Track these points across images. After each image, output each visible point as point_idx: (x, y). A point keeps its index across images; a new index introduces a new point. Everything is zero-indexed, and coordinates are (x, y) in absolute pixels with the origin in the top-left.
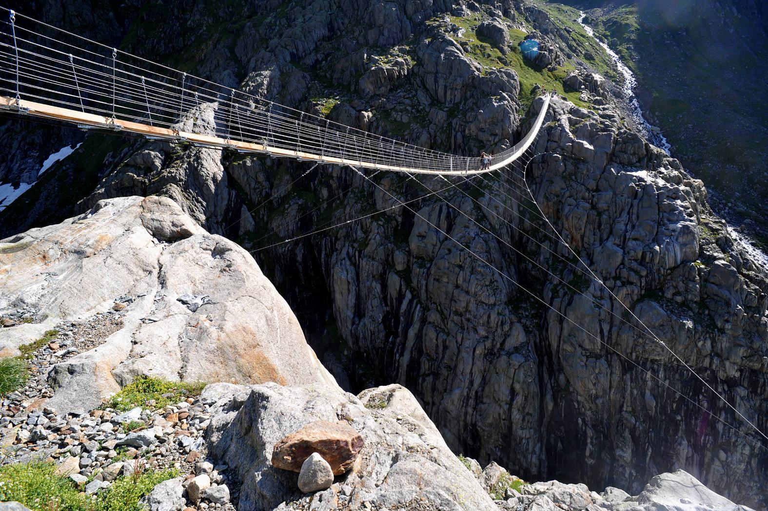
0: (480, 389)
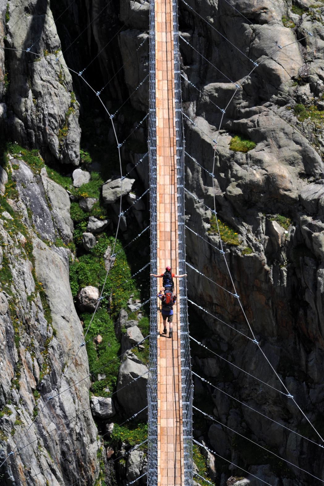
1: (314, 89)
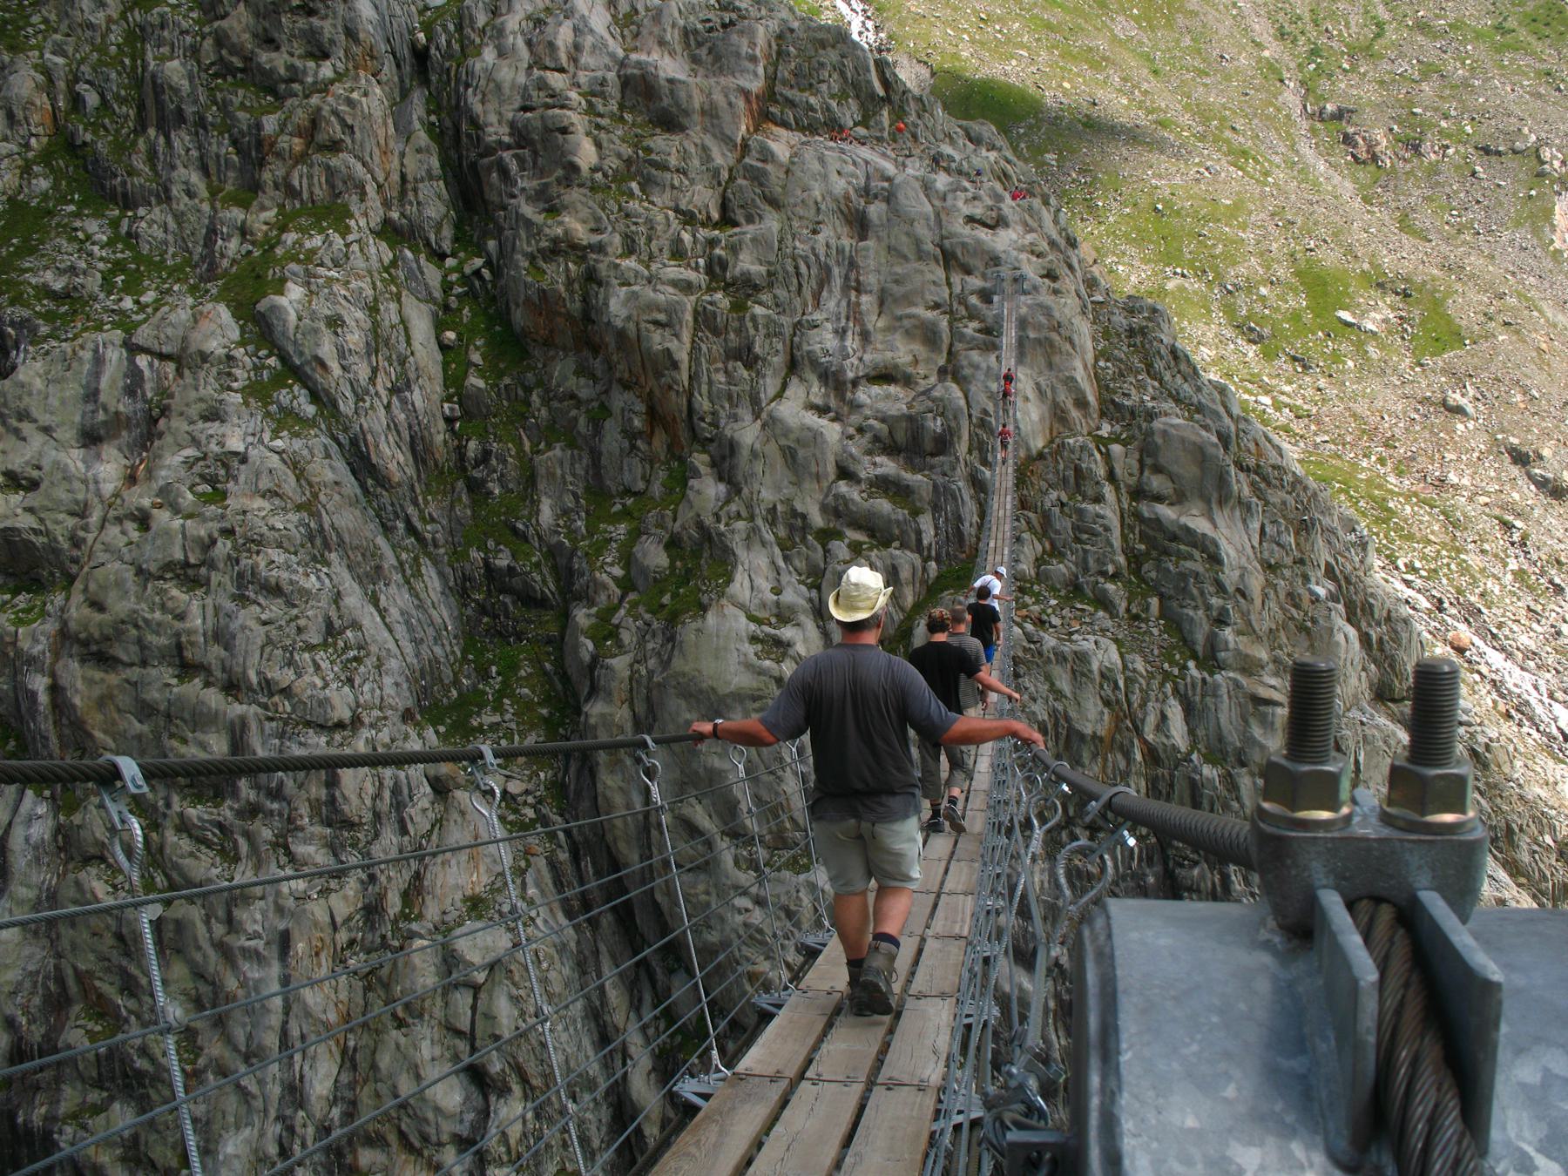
0: (336, 1113)
1: (605, 175)
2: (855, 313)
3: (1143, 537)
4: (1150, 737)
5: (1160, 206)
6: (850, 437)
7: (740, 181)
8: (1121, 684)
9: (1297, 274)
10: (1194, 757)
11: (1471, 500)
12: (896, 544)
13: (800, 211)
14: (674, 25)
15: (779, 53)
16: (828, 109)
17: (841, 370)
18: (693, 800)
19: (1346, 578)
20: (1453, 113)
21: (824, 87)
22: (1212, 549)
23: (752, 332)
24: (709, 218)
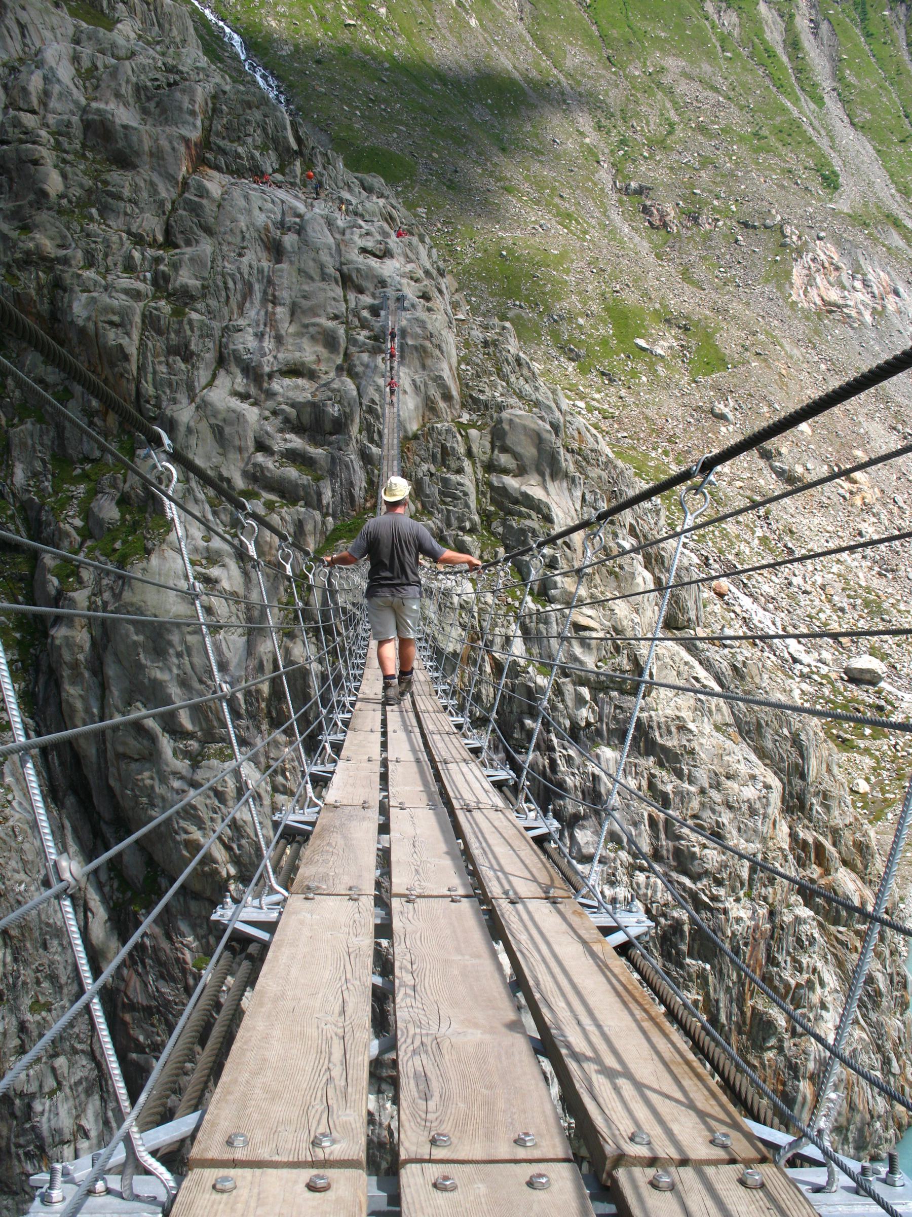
1: (70, 202)
2: (271, 320)
3: (493, 501)
4: (496, 655)
5: (504, 253)
6: (266, 419)
7: (181, 212)
8: (476, 614)
9: (607, 309)
10: (530, 669)
11: (730, 484)
12: (302, 503)
13: (229, 238)
14: (128, 82)
15: (214, 110)
16: (253, 158)
17: (260, 365)
18: (139, 704)
19: (644, 536)
20: (723, 195)
21: (249, 140)
22: (545, 511)
23: (189, 333)
24: (155, 240)
